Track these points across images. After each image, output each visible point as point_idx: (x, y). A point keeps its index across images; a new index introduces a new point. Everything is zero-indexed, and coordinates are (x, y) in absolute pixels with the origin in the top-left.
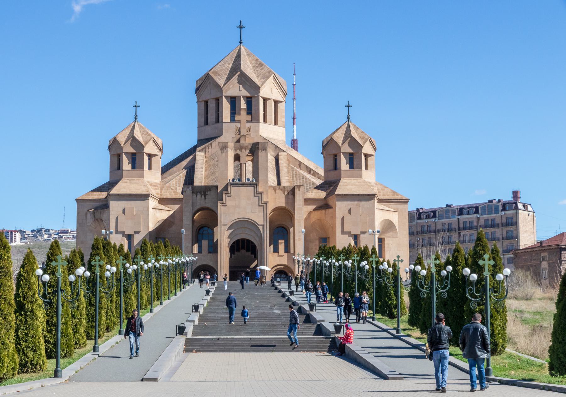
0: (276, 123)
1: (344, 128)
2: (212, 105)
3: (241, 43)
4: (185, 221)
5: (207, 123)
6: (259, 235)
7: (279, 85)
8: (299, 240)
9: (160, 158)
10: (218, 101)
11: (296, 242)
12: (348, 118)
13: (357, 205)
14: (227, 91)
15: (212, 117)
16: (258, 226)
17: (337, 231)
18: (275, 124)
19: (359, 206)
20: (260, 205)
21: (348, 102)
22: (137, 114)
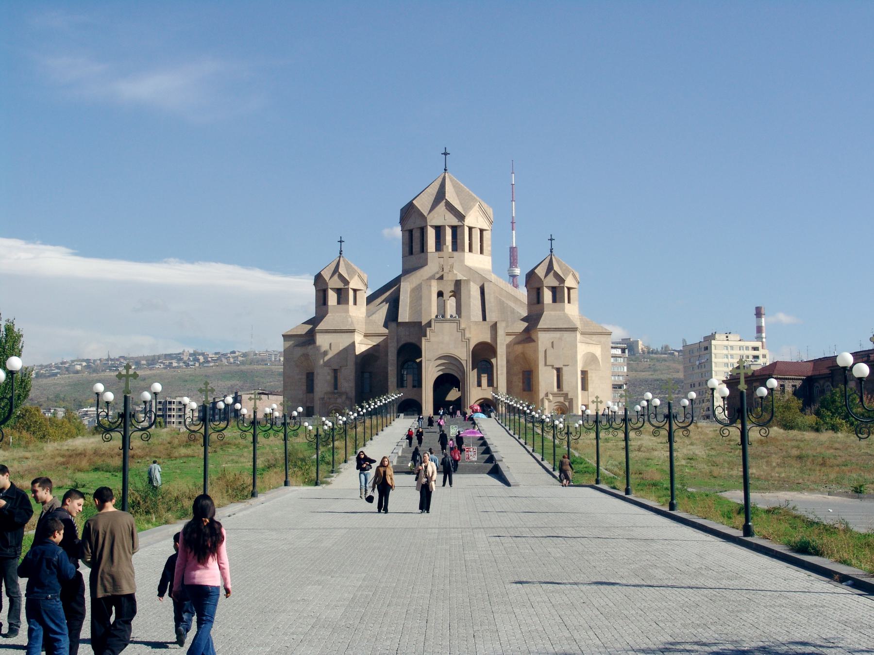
0: (482, 252)
1: (547, 262)
2: (417, 234)
4: (390, 356)
5: (411, 252)
7: (485, 213)
8: (502, 374)
10: (423, 231)
11: (498, 376)
12: (551, 252)
13: (560, 339)
14: (431, 220)
15: (416, 247)
16: (461, 361)
18: (481, 253)
19: (560, 339)
20: (463, 340)
21: (551, 235)
22: (342, 250)
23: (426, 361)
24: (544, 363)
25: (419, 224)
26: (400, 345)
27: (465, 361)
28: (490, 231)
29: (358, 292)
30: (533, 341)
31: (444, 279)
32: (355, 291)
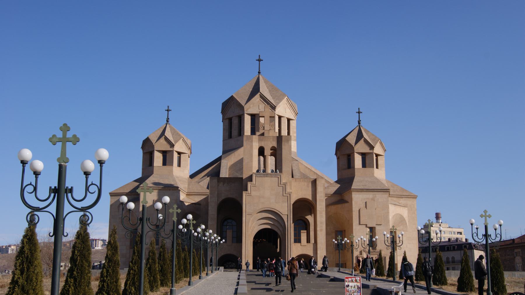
1: (356, 132)
2: (235, 122)
3: (259, 73)
5: (230, 137)
6: (283, 225)
7: (292, 106)
8: (321, 230)
9: (189, 157)
10: (241, 119)
12: (359, 123)
13: (373, 199)
14: (248, 109)
15: (235, 132)
17: (354, 224)
19: (373, 199)
20: (284, 195)
21: (359, 109)
22: (169, 117)
23: (247, 216)
24: (358, 222)
25: (237, 112)
26: (221, 200)
27: (286, 216)
28: (295, 121)
29: (182, 155)
30: (347, 202)
31: (265, 135)
32: (179, 153)
